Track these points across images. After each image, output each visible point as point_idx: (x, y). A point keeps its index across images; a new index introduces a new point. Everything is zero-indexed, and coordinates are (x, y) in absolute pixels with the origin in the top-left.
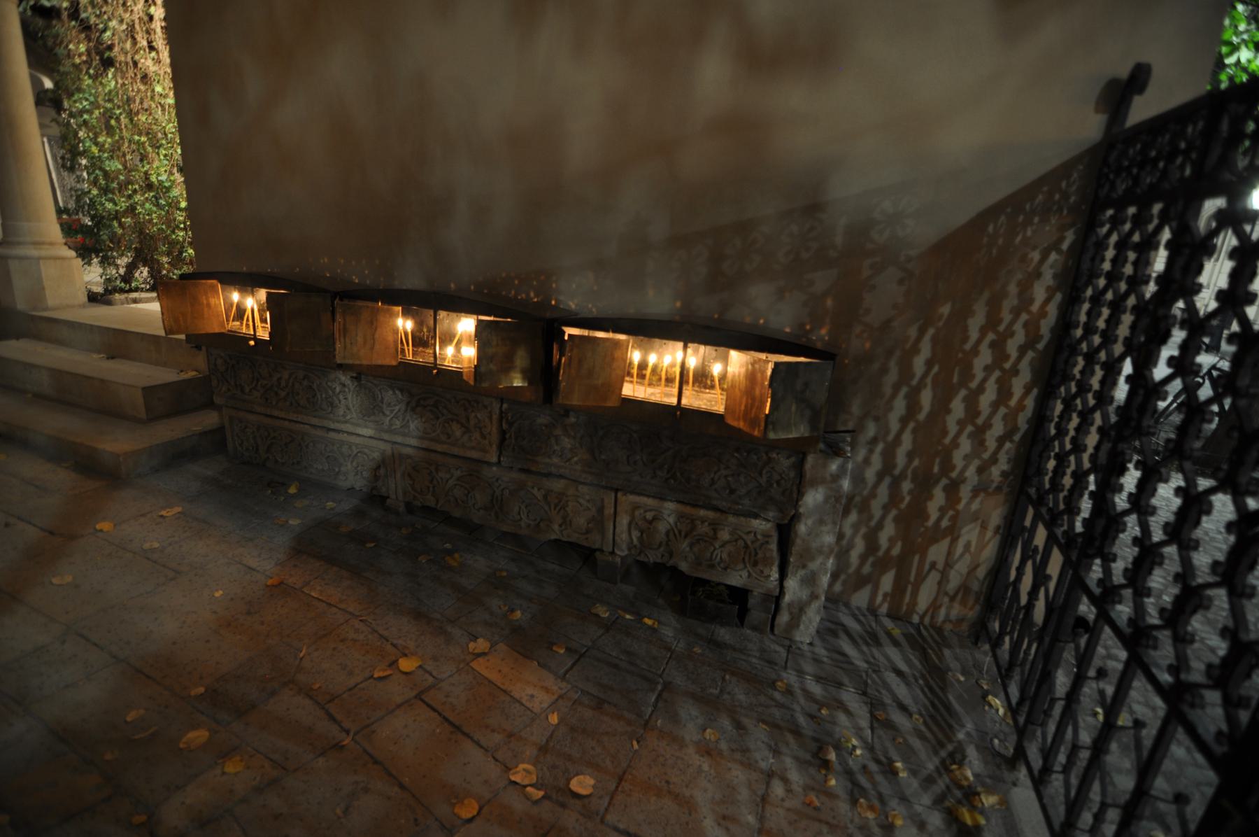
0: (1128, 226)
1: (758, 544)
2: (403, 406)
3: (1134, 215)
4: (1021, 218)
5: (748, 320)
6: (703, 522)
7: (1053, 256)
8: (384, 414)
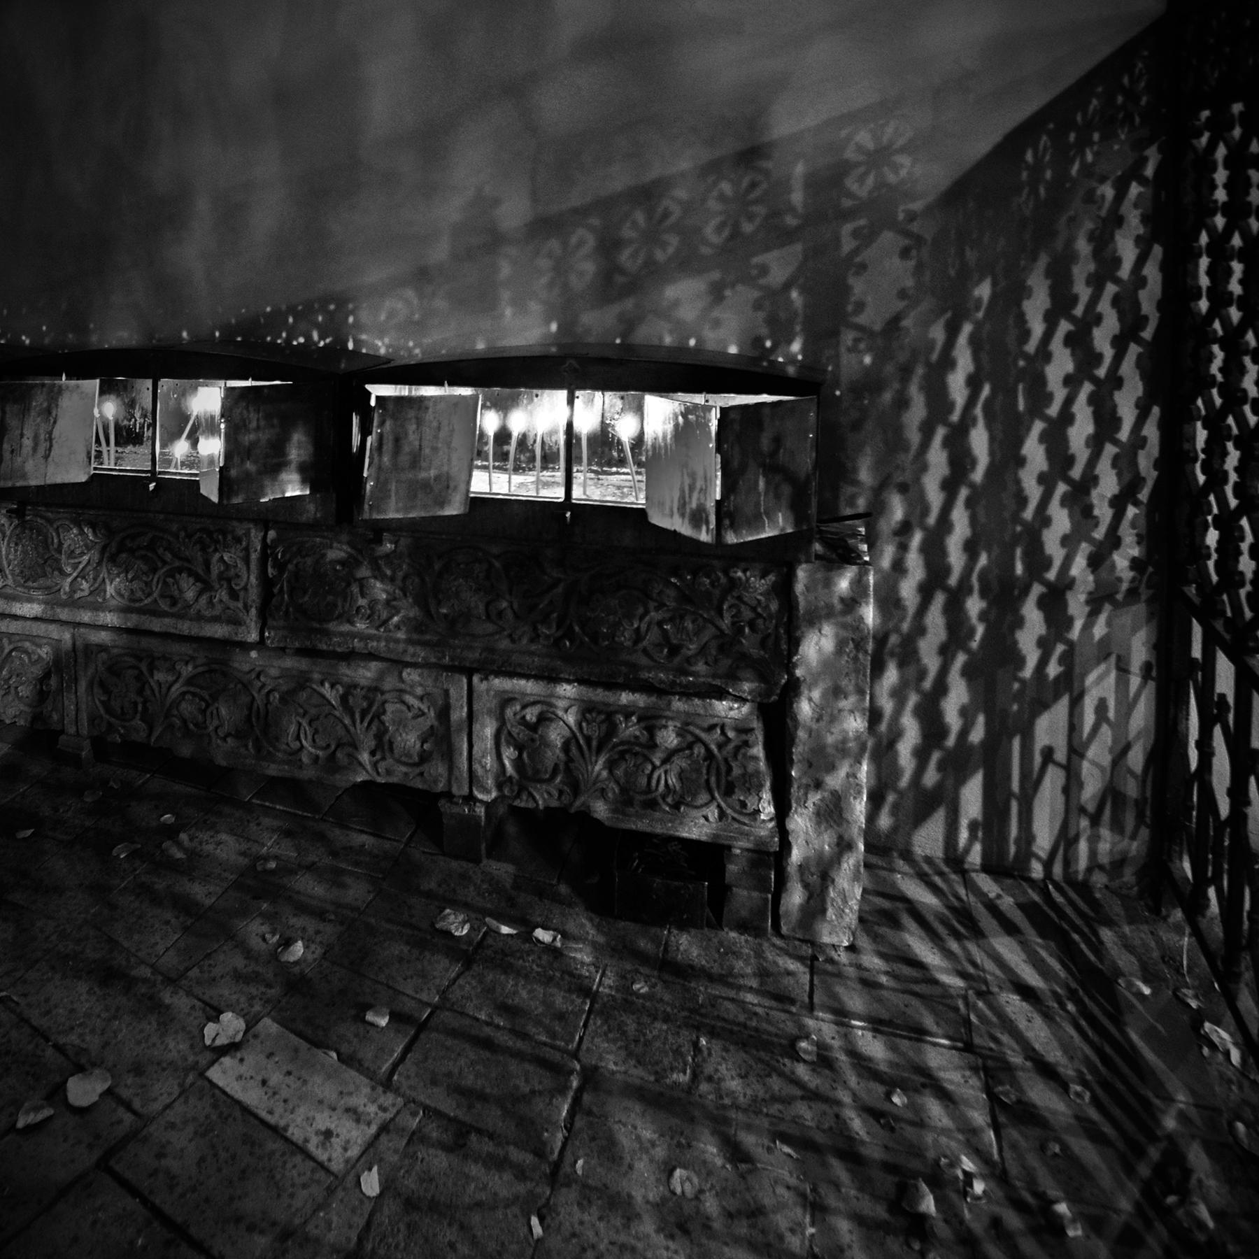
0: (1237, 132)
1: (731, 746)
2: (94, 555)
3: (1241, 113)
4: (1072, 137)
5: (668, 340)
6: (627, 717)
7: (1135, 189)
8: (63, 574)
